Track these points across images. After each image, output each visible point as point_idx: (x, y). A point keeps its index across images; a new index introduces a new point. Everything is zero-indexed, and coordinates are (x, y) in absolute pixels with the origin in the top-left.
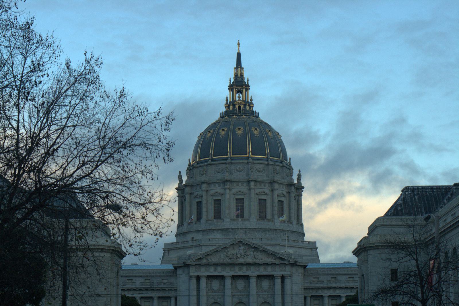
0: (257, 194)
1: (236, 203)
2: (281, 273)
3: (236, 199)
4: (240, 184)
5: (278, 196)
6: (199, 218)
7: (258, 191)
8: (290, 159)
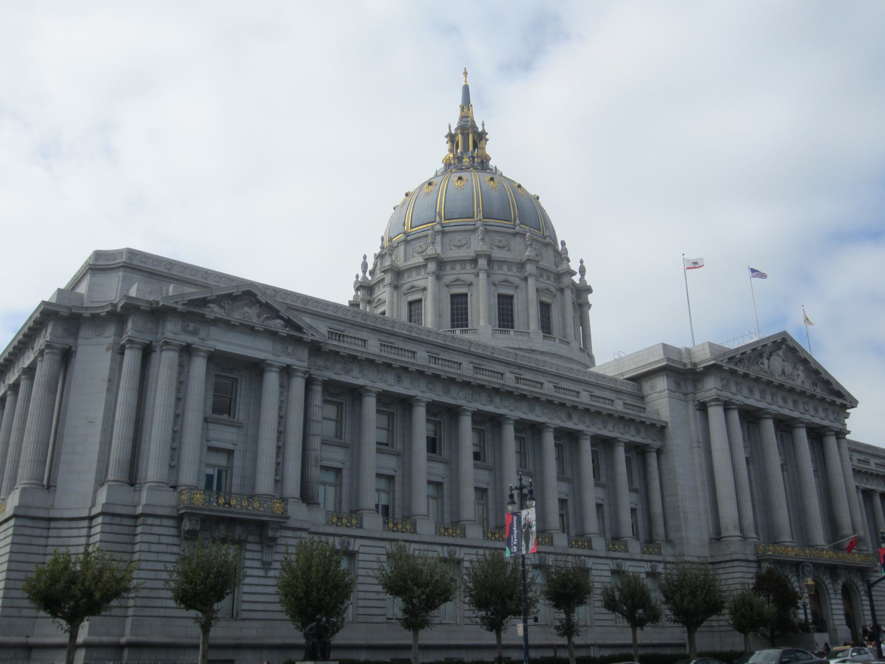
0: (494, 284)
1: (452, 304)
3: (453, 296)
4: (458, 267)
5: (537, 290)
7: (497, 278)
8: (563, 243)
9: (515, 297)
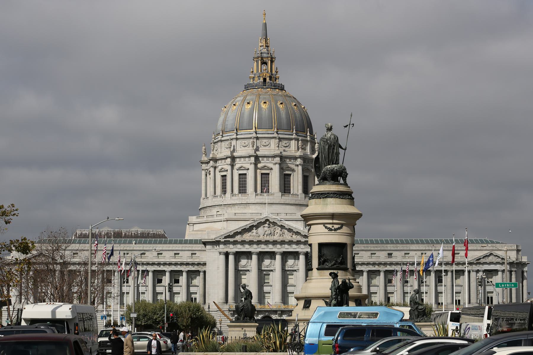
6: (224, 191)
9: (292, 175)
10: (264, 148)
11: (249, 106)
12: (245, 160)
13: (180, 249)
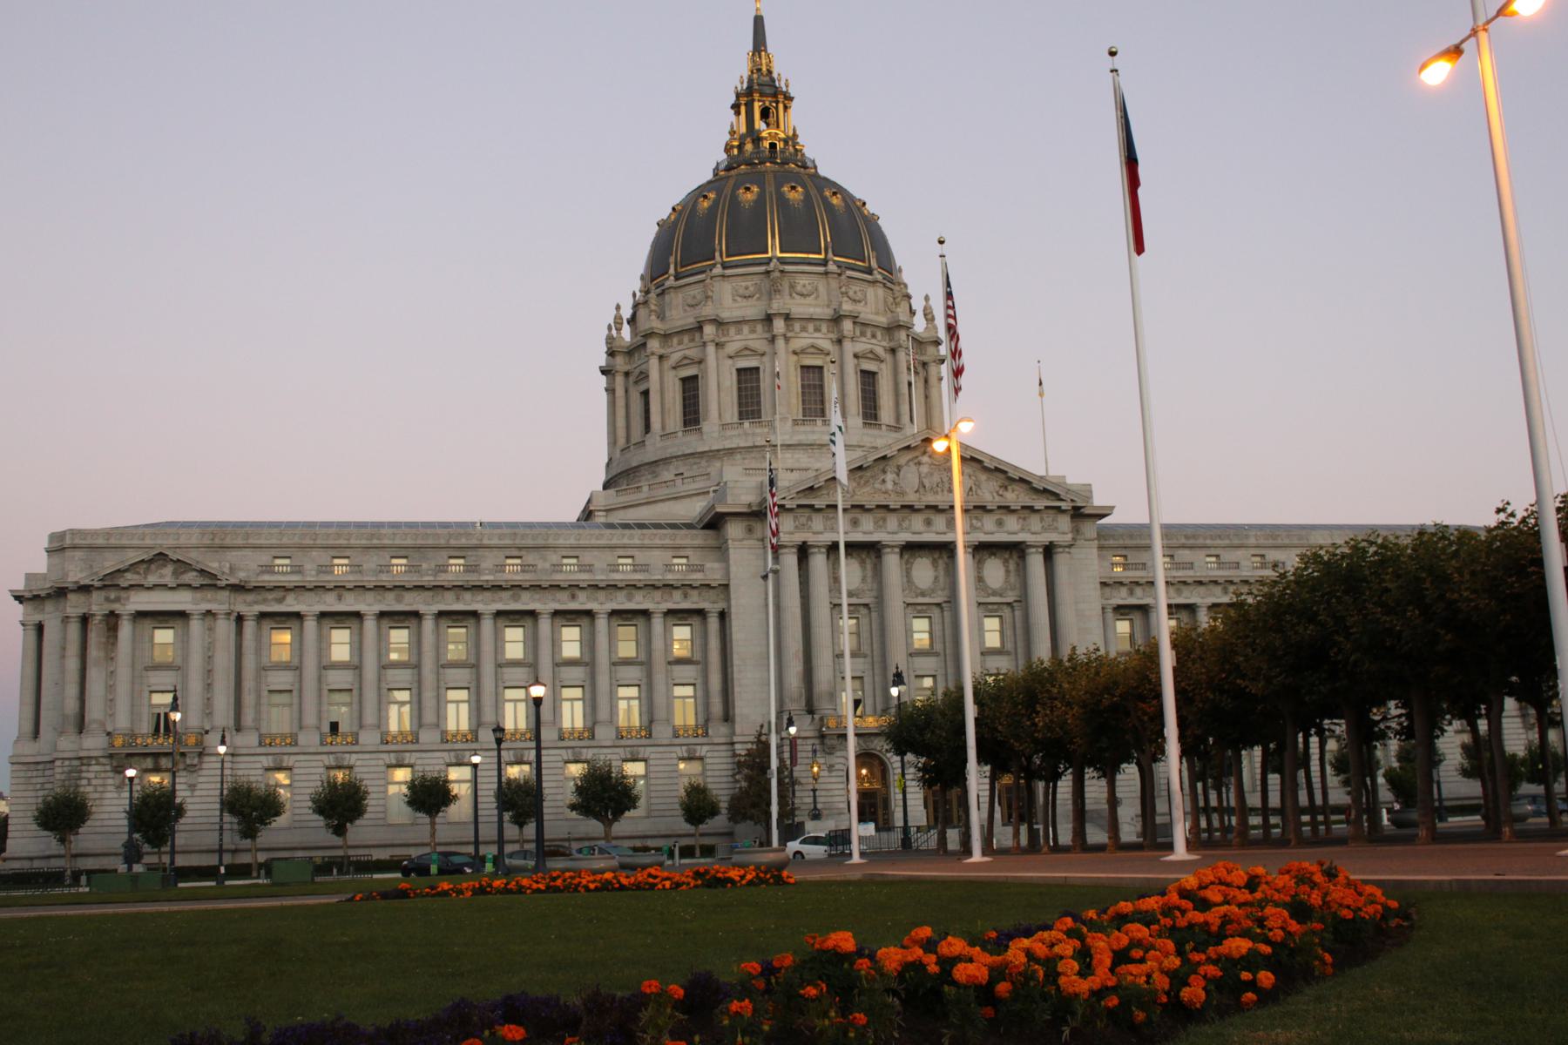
2: (1046, 538)
7: (860, 347)
10: (802, 300)
11: (749, 196)
12: (753, 331)
13: (637, 542)
